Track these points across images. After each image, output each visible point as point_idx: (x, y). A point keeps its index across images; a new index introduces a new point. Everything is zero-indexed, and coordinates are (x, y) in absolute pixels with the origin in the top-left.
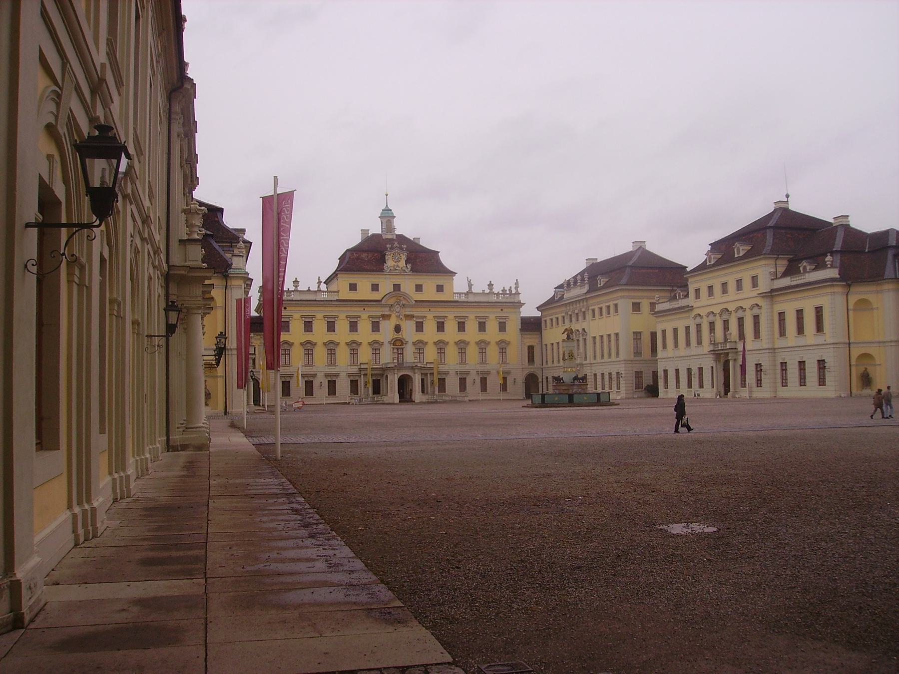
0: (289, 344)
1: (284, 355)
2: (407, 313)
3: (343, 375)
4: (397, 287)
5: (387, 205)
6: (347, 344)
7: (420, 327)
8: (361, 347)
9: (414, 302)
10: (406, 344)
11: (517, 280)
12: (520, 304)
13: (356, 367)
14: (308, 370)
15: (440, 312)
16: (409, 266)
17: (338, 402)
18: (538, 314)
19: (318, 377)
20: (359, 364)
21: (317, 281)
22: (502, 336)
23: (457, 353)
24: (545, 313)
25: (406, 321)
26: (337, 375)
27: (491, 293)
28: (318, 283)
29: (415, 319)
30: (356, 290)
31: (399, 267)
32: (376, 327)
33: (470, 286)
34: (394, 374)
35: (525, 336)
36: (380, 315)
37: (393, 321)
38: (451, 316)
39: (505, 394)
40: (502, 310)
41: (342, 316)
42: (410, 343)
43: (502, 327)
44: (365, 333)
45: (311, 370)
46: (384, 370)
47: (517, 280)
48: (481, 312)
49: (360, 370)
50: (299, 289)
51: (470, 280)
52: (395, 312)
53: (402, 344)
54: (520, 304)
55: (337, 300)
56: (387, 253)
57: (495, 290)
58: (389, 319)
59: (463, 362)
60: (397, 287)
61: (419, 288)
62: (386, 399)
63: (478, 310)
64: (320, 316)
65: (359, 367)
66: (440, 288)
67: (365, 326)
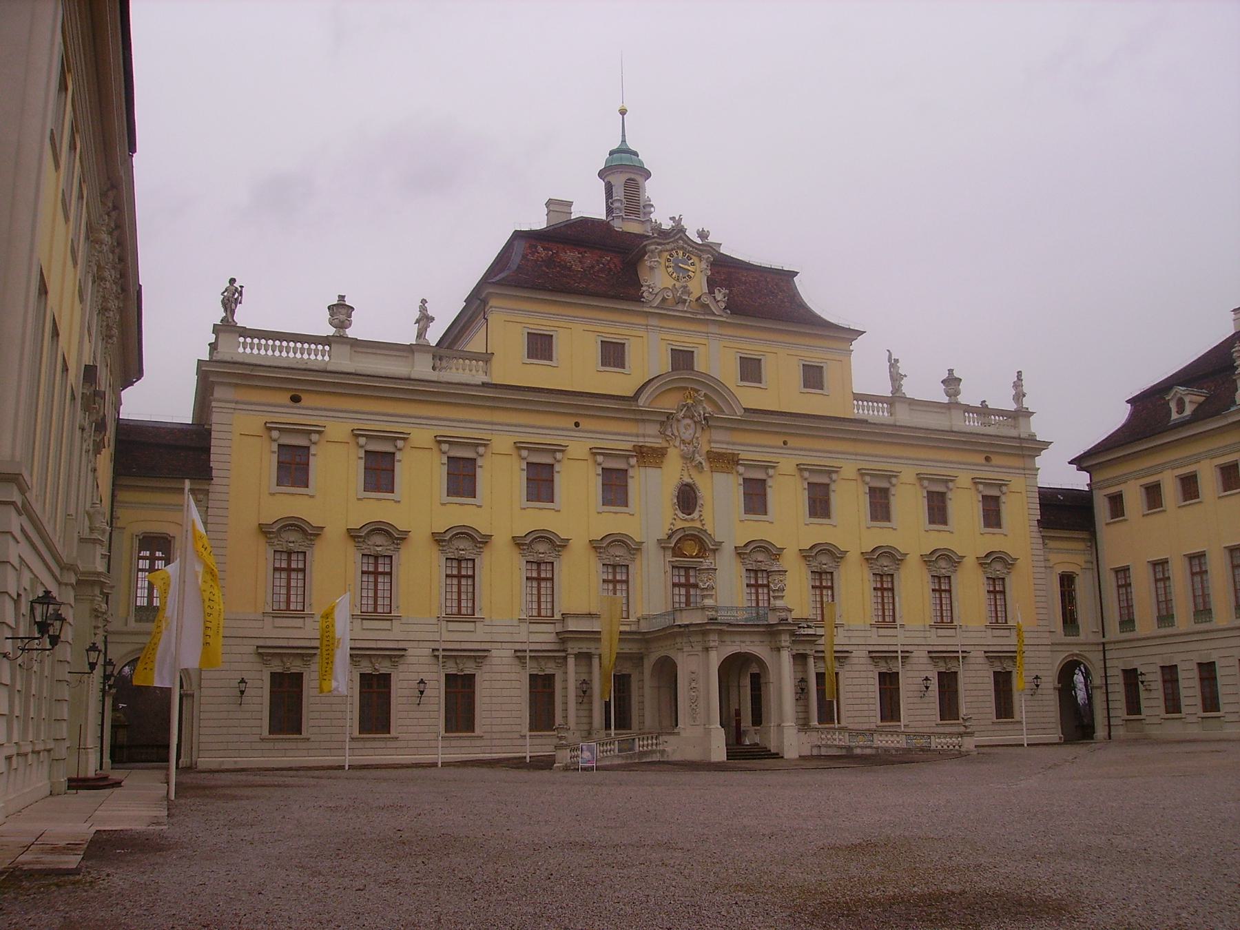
0: (304, 531)
1: (284, 575)
2: (718, 447)
3: (502, 656)
4: (682, 359)
6: (518, 542)
8: (565, 556)
9: (740, 412)
10: (714, 551)
11: (1019, 373)
12: (1031, 448)
13: (550, 628)
14: (381, 634)
15: (818, 453)
16: (719, 297)
17: (480, 756)
18: (1079, 481)
19: (410, 660)
20: (557, 616)
21: (417, 315)
23: (869, 594)
24: (1101, 476)
25: (715, 474)
26: (480, 656)
27: (953, 405)
28: (418, 322)
29: (741, 469)
30: (550, 358)
31: (689, 294)
33: (896, 378)
34: (707, 649)
35: (1051, 544)
36: (629, 446)
37: (672, 473)
38: (849, 469)
39: (1010, 727)
40: (987, 459)
41: (502, 442)
42: (727, 552)
43: (992, 514)
45: (383, 635)
46: (647, 641)
47: (1019, 373)
49: (564, 638)
50: (350, 333)
51: (897, 361)
52: (677, 444)
54: (1031, 448)
55: (484, 385)
56: (653, 247)
57: (968, 396)
59: (887, 620)
60: (682, 359)
61: (751, 370)
62: (676, 747)
63: (932, 454)
64: (422, 436)
65: (559, 628)
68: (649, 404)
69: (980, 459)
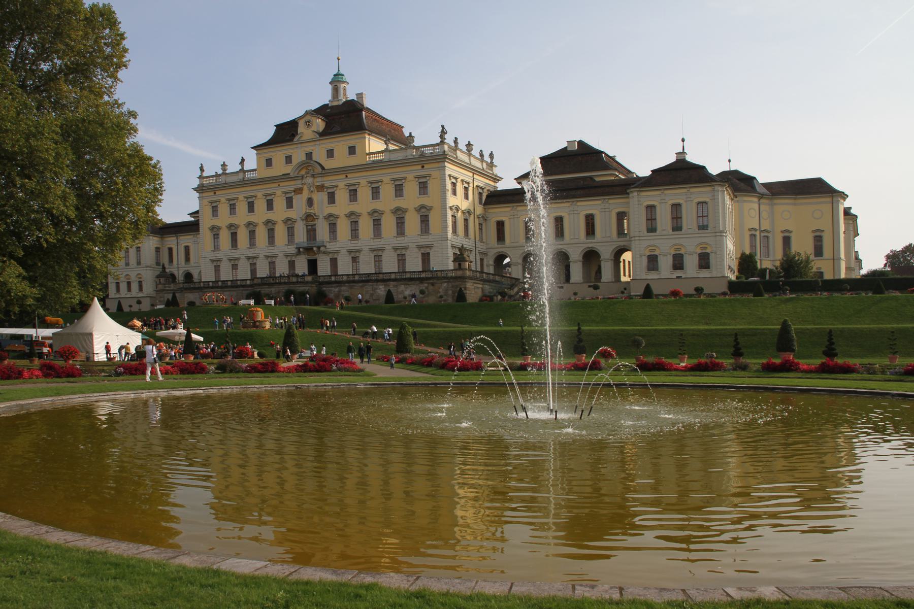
4: (309, 155)
5: (339, 70)
7: (332, 198)
22: (425, 201)
29: (325, 190)
32: (290, 203)
37: (305, 194)
40: (423, 167)
44: (280, 212)
48: (398, 172)
53: (314, 220)
58: (301, 193)
60: (309, 155)
61: (330, 154)
66: (352, 150)
67: (280, 203)
68: (298, 174)
69: (420, 167)
